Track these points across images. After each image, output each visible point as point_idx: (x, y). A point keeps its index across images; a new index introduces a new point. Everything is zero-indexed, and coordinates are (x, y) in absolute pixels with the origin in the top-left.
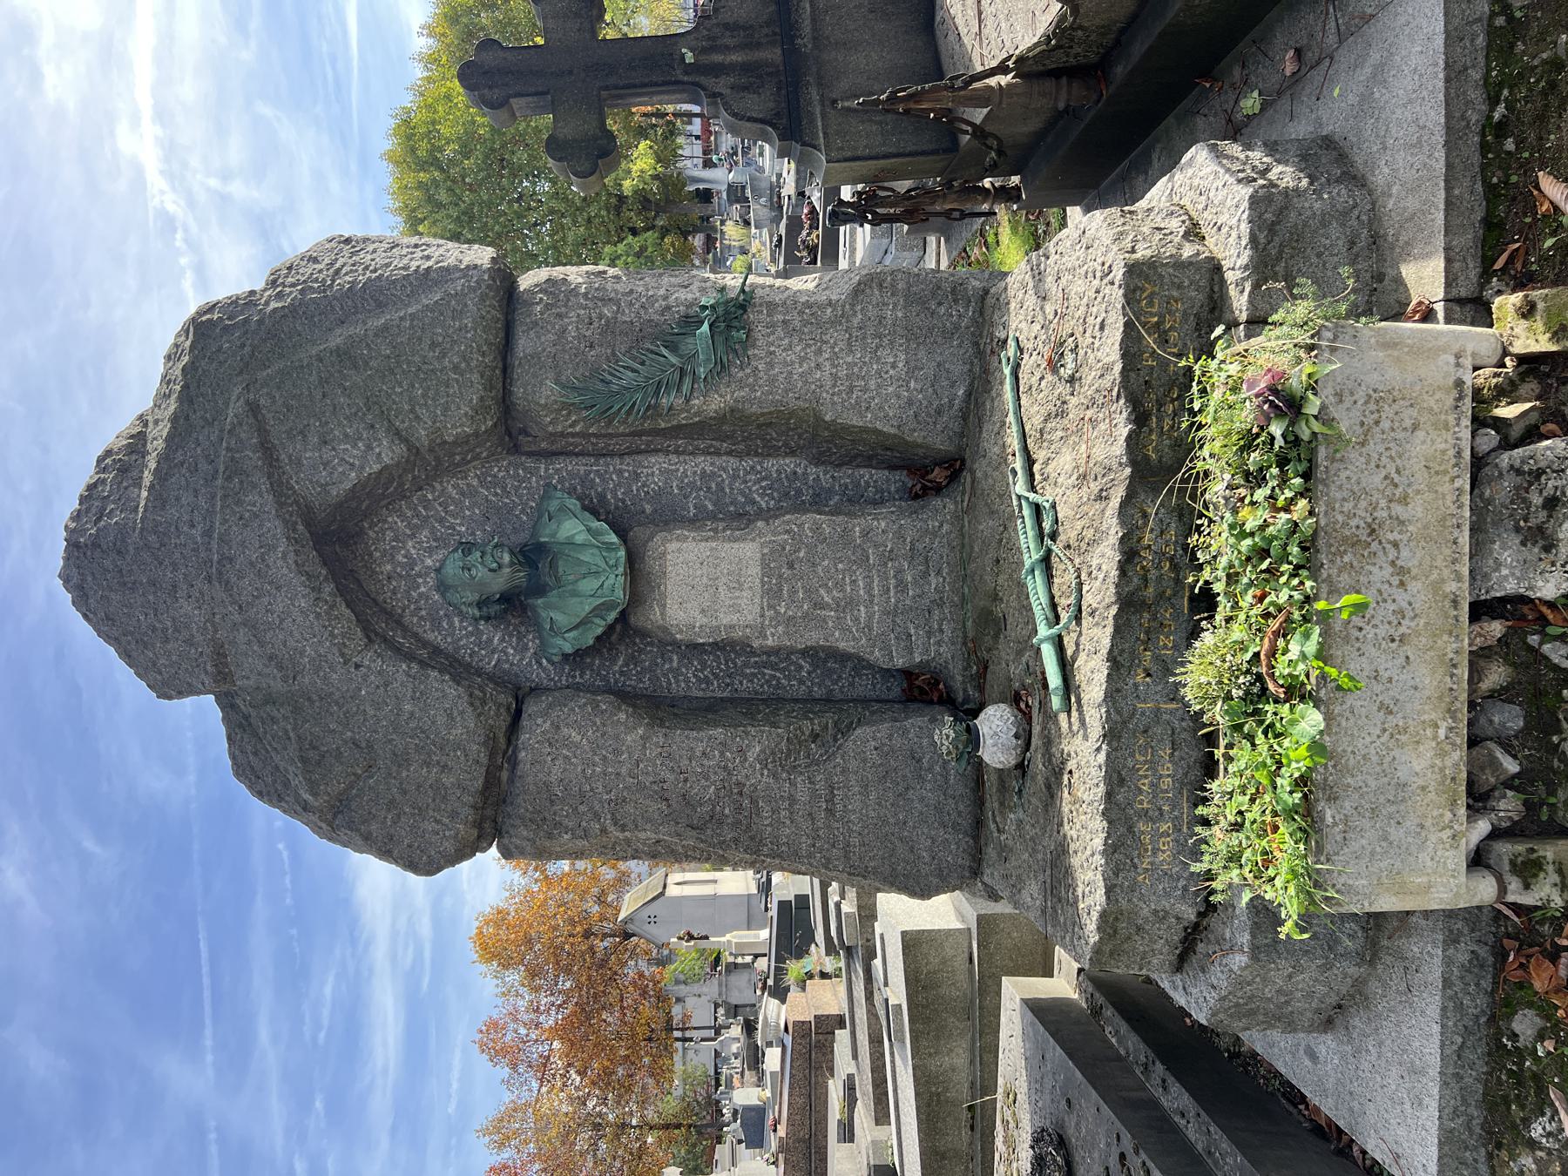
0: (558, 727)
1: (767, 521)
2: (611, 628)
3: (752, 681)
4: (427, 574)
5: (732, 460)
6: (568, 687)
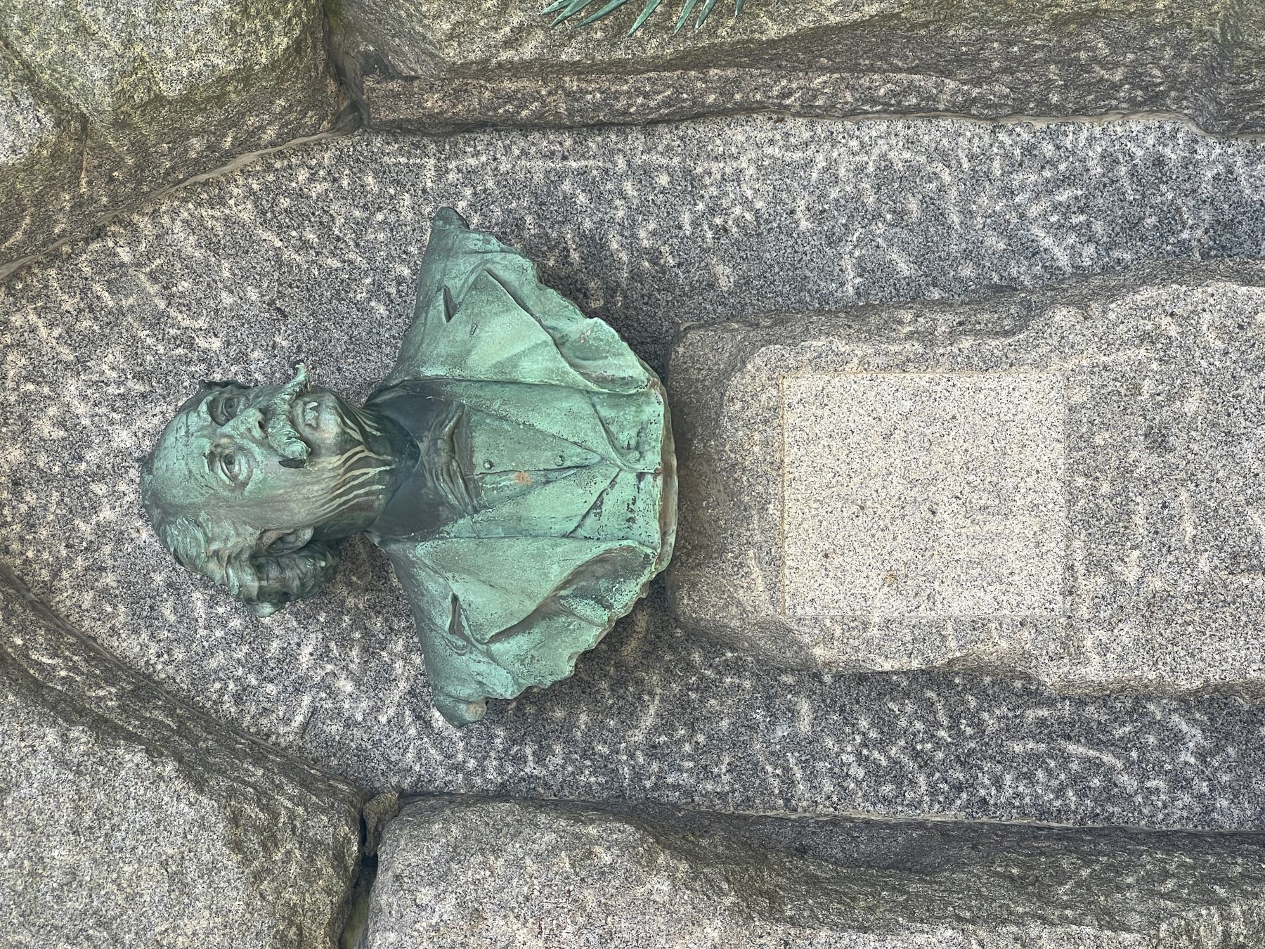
0: (477, 915)
1: (1081, 305)
2: (620, 629)
3: (1030, 778)
4: (118, 472)
5: (968, 127)
6: (502, 794)
